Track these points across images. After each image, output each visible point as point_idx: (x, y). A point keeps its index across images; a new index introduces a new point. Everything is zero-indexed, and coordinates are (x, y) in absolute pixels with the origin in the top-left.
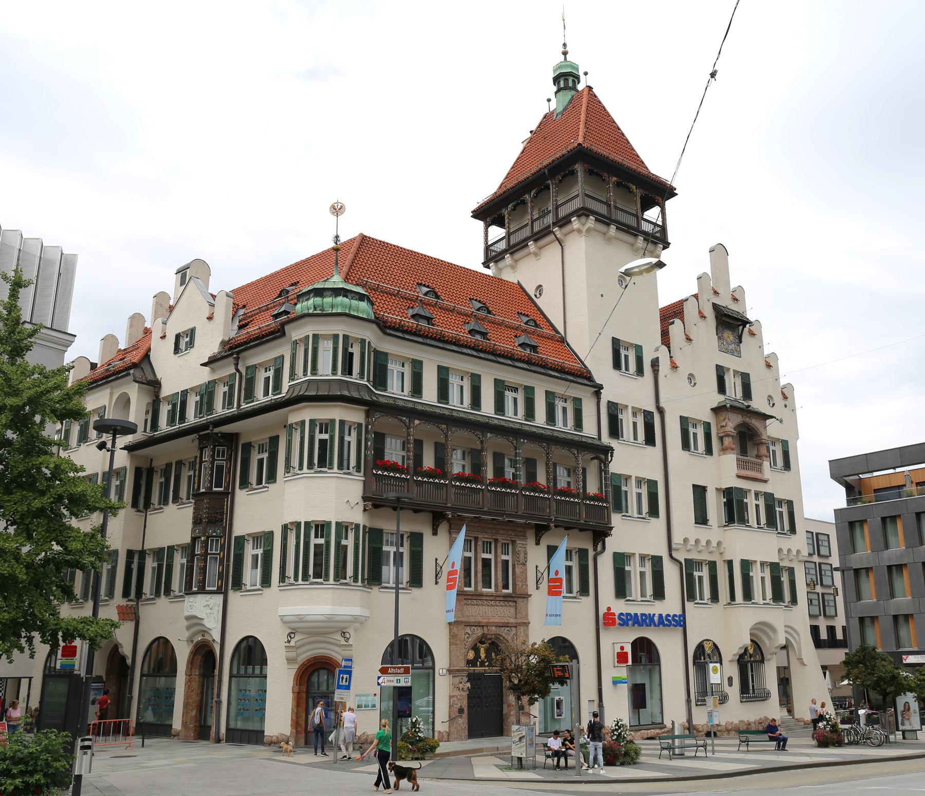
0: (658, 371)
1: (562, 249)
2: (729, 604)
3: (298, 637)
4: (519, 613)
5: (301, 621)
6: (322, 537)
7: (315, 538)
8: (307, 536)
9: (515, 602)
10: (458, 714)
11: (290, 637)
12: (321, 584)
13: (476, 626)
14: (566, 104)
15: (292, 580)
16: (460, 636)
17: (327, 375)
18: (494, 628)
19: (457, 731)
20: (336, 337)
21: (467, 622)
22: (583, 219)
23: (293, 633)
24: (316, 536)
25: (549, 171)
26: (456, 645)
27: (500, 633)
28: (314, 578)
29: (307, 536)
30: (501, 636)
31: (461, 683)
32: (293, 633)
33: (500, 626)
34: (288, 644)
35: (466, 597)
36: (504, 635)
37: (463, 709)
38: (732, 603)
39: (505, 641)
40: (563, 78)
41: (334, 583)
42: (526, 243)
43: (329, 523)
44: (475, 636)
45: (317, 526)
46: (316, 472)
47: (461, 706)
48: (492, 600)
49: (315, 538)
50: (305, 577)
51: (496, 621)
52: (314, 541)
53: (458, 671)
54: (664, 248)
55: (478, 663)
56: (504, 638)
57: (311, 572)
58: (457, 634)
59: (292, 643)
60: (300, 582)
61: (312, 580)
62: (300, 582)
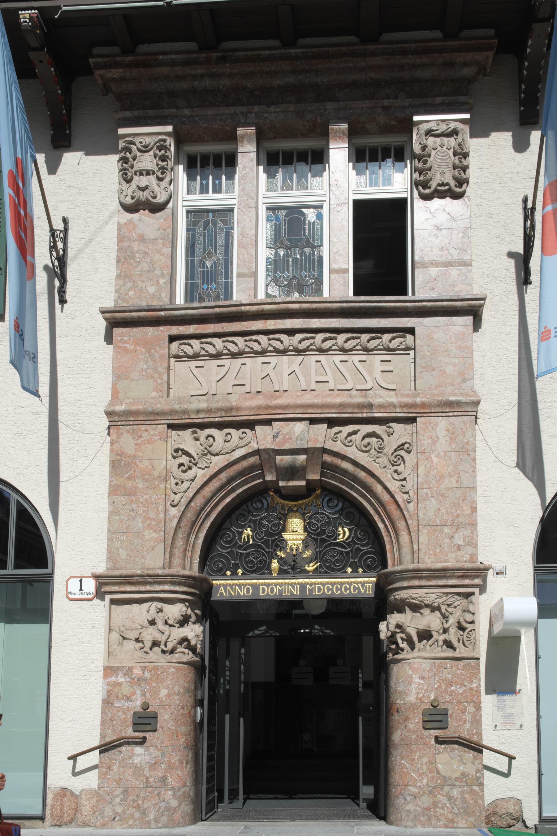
4: (430, 368)
9: (411, 331)
10: (130, 732)
13: (220, 426)
16: (146, 463)
18: (299, 427)
19: (126, 792)
21: (172, 412)
26: (131, 493)
27: (338, 447)
30: (344, 458)
31: (152, 623)
33: (332, 422)
35: (176, 330)
36: (352, 452)
37: (155, 717)
39: (362, 475)
44: (218, 462)
47: (146, 707)
48: (291, 332)
51: (308, 399)
53: (128, 579)
55: (275, 565)
56: (355, 463)
58: (133, 458)
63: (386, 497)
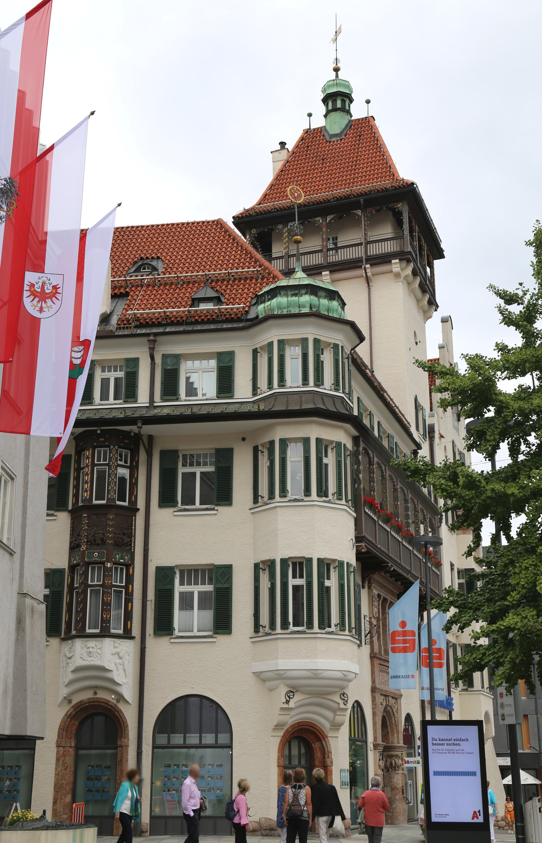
0: (434, 437)
1: (369, 289)
2: (466, 690)
3: (297, 698)
5: (317, 677)
6: (301, 576)
7: (293, 578)
8: (284, 576)
11: (289, 697)
12: (303, 632)
14: (343, 127)
15: (267, 629)
17: (298, 387)
20: (304, 341)
22: (404, 264)
23: (292, 692)
24: (294, 577)
25: (365, 201)
28: (294, 626)
29: (284, 576)
32: (292, 692)
34: (285, 706)
38: (469, 689)
40: (341, 98)
41: (318, 631)
42: (319, 271)
43: (310, 560)
45: (294, 564)
46: (290, 501)
49: (293, 578)
50: (285, 625)
52: (292, 582)
54: (436, 310)
57: (291, 619)
59: (292, 704)
60: (279, 630)
61: (292, 628)
62: (279, 630)
63: (394, 722)
